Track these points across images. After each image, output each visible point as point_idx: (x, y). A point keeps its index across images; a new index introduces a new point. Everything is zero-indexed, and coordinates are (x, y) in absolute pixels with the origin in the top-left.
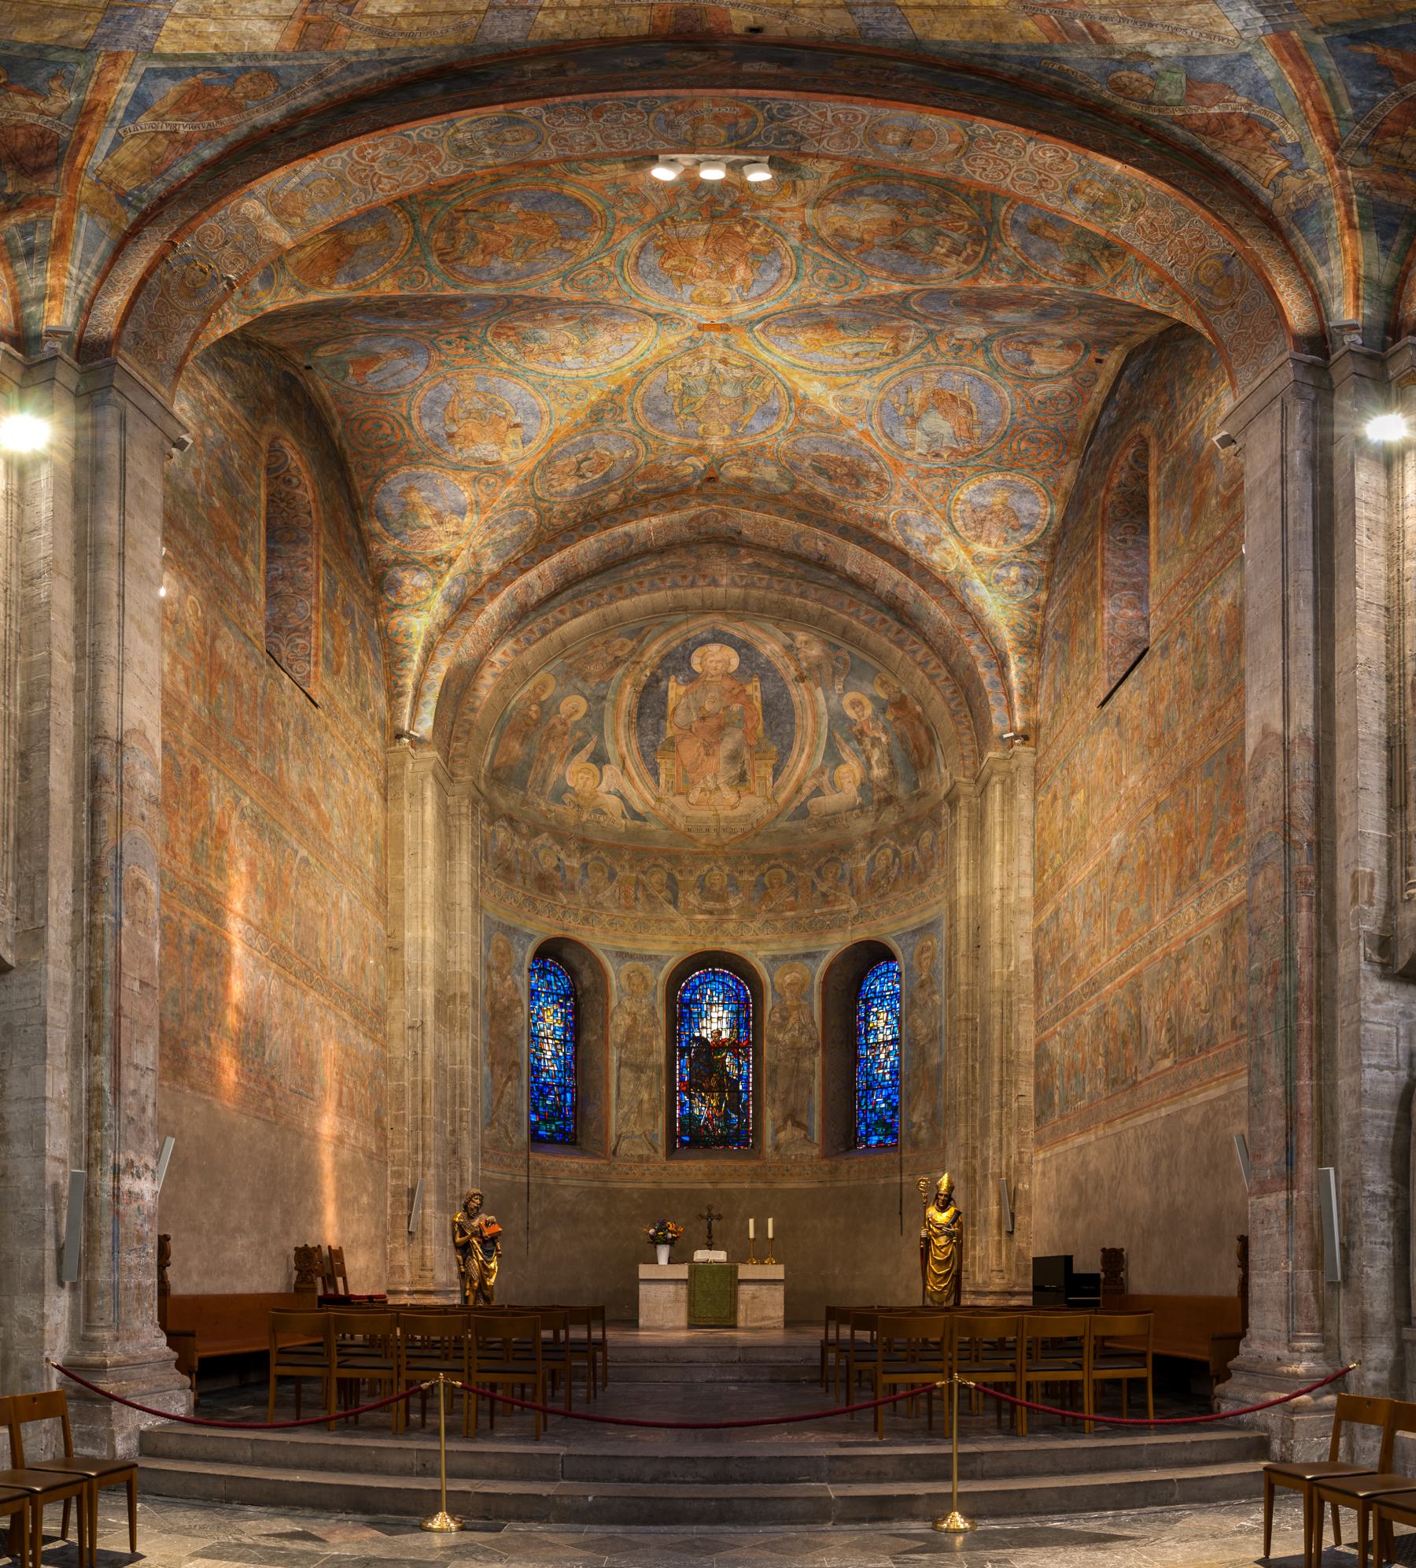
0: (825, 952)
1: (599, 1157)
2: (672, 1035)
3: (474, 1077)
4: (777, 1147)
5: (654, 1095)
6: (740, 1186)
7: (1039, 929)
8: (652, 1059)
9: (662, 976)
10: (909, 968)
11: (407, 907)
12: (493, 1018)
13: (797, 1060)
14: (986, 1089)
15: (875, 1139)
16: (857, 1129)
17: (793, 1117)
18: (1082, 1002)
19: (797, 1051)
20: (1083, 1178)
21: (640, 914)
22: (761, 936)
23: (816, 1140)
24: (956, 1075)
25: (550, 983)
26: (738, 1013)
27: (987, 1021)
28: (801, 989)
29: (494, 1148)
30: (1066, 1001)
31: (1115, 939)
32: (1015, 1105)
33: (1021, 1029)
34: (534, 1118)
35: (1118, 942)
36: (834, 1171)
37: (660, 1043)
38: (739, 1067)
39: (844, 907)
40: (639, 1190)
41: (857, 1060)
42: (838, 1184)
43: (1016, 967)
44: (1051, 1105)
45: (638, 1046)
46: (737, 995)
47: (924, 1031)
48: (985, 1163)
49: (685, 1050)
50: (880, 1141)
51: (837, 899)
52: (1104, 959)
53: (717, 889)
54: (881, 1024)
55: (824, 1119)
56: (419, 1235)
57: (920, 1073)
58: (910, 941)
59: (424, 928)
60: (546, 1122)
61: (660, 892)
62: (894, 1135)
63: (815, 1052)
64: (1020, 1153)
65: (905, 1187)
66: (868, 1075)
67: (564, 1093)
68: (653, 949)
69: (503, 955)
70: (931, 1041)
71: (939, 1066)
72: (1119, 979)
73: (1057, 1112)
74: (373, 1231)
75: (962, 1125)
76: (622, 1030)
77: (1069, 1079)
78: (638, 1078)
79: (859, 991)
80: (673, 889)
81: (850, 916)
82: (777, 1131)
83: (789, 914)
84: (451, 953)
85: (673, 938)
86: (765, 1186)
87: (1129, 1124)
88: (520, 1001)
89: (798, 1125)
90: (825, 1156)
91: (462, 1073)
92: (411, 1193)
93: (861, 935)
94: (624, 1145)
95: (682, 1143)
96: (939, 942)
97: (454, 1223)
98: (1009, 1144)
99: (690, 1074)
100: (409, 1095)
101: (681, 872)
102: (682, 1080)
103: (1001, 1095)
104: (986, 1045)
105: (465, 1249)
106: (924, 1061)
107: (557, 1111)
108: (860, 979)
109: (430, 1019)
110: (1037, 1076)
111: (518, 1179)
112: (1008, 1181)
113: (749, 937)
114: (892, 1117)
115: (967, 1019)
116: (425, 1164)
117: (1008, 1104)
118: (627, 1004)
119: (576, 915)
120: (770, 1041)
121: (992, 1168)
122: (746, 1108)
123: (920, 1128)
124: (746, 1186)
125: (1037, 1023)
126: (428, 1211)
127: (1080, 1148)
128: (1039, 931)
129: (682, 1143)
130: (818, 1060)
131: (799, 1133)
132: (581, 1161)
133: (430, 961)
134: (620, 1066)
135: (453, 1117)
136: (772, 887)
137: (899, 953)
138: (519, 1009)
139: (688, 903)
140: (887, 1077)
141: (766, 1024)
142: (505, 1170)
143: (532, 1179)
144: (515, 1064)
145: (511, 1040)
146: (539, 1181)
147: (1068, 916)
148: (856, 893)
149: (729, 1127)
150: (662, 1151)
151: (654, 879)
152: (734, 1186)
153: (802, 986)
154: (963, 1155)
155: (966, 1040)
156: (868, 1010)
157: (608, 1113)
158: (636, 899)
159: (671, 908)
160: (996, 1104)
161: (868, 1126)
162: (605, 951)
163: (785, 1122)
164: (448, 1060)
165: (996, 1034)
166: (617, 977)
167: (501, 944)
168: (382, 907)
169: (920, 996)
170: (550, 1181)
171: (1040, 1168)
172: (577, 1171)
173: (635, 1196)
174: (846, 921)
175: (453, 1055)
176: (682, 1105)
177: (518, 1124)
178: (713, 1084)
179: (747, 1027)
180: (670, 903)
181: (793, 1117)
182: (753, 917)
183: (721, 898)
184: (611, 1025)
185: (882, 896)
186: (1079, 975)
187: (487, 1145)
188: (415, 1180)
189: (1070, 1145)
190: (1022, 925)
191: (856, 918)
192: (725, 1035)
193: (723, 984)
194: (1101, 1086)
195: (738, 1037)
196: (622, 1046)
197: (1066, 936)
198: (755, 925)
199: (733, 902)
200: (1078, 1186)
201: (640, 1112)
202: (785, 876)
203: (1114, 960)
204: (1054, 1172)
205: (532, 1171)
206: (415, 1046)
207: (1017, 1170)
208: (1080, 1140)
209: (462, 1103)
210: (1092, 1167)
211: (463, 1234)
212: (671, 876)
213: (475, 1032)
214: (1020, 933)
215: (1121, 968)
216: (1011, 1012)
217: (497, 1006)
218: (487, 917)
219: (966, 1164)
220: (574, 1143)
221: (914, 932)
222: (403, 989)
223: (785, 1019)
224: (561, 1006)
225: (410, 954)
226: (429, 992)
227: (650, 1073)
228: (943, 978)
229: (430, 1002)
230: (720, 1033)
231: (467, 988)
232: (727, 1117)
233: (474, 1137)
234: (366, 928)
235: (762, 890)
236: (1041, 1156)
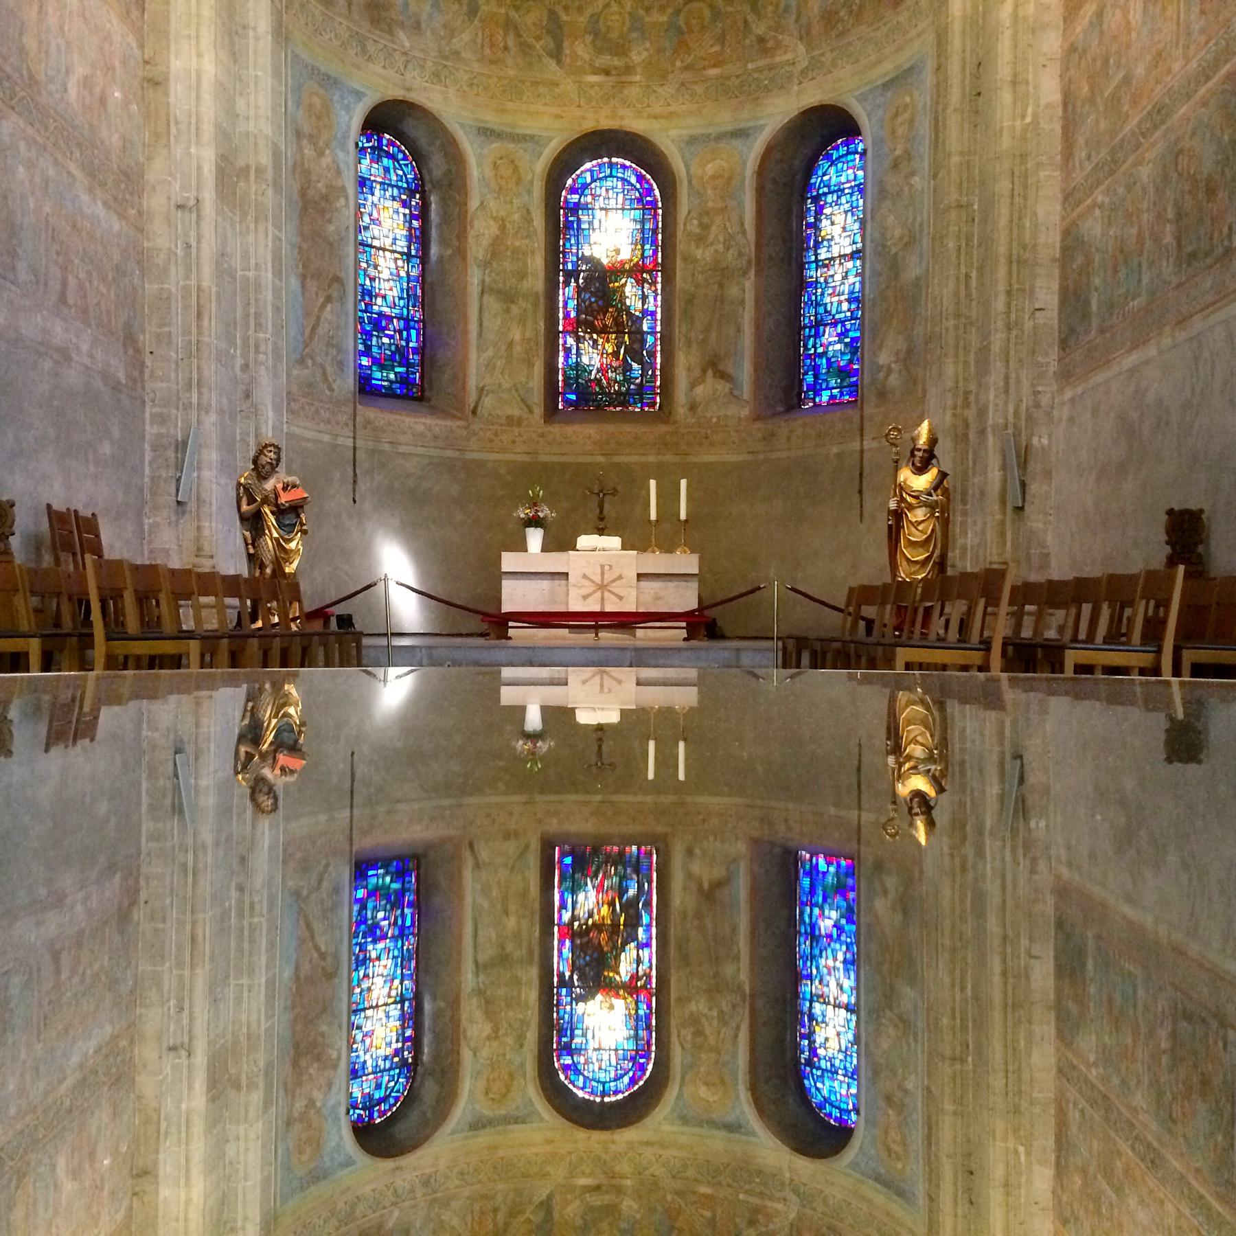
0: (762, 127)
1: (454, 417)
2: (554, 254)
3: (276, 291)
4: (693, 407)
5: (528, 335)
6: (642, 459)
7: (1072, 49)
8: (525, 285)
9: (541, 165)
10: (878, 142)
11: (173, 17)
12: (304, 209)
13: (721, 286)
14: (986, 304)
15: (825, 396)
16: (801, 381)
17: (714, 366)
18: (1139, 145)
19: (722, 273)
20: (1134, 415)
21: (511, 72)
22: (674, 107)
23: (746, 397)
24: (944, 291)
25: (387, 170)
26: (643, 222)
27: (988, 205)
28: (727, 182)
29: (306, 395)
30: (1113, 152)
31: (1196, 27)
32: (1028, 325)
33: (1041, 212)
34: (365, 361)
35: (1202, 31)
36: (769, 438)
37: (538, 263)
38: (644, 298)
39: (788, 57)
40: (507, 462)
41: (802, 284)
42: (774, 456)
43: (1035, 115)
44: (1086, 316)
45: (507, 265)
46: (640, 200)
47: (897, 233)
48: (982, 413)
49: (572, 275)
50: (832, 397)
51: (778, 44)
52: (1177, 66)
53: (614, 35)
54: (837, 230)
55: (756, 367)
56: (192, 506)
57: (890, 294)
58: (880, 100)
59: (199, 55)
60: (382, 367)
61: (538, 38)
62: (854, 389)
63: (745, 273)
64: (1036, 393)
65: (867, 455)
66: (818, 304)
67: (407, 328)
68: (529, 126)
69: (319, 118)
70: (906, 245)
71: (918, 279)
72: (1202, 91)
73: (1095, 322)
74: (120, 497)
75: (949, 361)
76: (485, 242)
77: (1115, 271)
78: (508, 311)
79: (807, 186)
80: (556, 30)
81: (799, 68)
82: (693, 385)
83: (713, 72)
84: (241, 105)
85: (555, 110)
86: (677, 459)
87: (1215, 318)
88: (343, 189)
89: (722, 375)
90: (758, 418)
91: (258, 285)
92: (181, 446)
93: (813, 96)
94: (488, 402)
95: (568, 402)
96: (922, 97)
97: (239, 484)
98: (1018, 382)
99: (578, 309)
100: (178, 306)
101: (566, 8)
102: (567, 315)
103: (1008, 312)
104: (986, 243)
105: (254, 523)
106: (897, 275)
107: (400, 355)
108: (810, 169)
109: (209, 196)
110: (1064, 277)
111: (340, 441)
112: (1017, 434)
113: (657, 109)
114: (851, 362)
115: (960, 206)
116: (203, 408)
117: (1018, 324)
118: (492, 204)
119: (423, 67)
120: (685, 259)
121: (992, 418)
122: (652, 354)
123: (889, 371)
124: (652, 459)
125: (1066, 198)
126: (206, 474)
127: (1132, 371)
128: (1072, 51)
129: (568, 402)
130: (749, 284)
131: (722, 387)
132: (428, 421)
133: (209, 110)
134: (483, 293)
135: (245, 344)
136: (691, 31)
137: (864, 122)
138: (342, 201)
139: (575, 56)
140: (845, 306)
141: (680, 235)
142: (322, 426)
143: (359, 443)
144: (337, 280)
145: (331, 245)
146: (371, 444)
147: (1118, 13)
148: (805, 35)
149: (628, 380)
150: (539, 411)
151: (531, 18)
152: (634, 459)
153: (730, 178)
154: (950, 403)
155: (959, 238)
156: (819, 211)
157: (465, 358)
158: (506, 48)
159: (553, 63)
160: (1000, 324)
161: (816, 377)
162: (462, 125)
163: (704, 371)
164: (237, 263)
165: (1003, 222)
166: (479, 165)
167: (317, 101)
168: (135, 14)
169: (892, 180)
170: (387, 447)
171: (1066, 412)
172: (422, 435)
173: (502, 471)
174: (790, 79)
175: (245, 255)
176: (568, 351)
177: (341, 365)
178: (609, 322)
179: (654, 242)
180: (551, 56)
181: (714, 366)
182: (664, 76)
183: (621, 49)
184: (471, 234)
185: (841, 35)
186: (1135, 103)
187: (295, 389)
188: (186, 430)
189: (1116, 369)
190: (1045, 49)
191: (804, 72)
192: (626, 254)
193: (623, 180)
194: (1167, 269)
195: (643, 257)
196: (486, 265)
197: (1114, 47)
198: (666, 91)
199: (638, 56)
200: (1128, 430)
201: (509, 357)
202: (707, 13)
203: (1194, 64)
204: (1088, 415)
205: (359, 433)
206: (186, 235)
207: (1030, 418)
208: (1133, 359)
209: (259, 327)
210: (1151, 396)
211: (251, 500)
212: (552, 14)
213: (277, 226)
214: (1042, 60)
215: (1205, 74)
216: (1025, 187)
217: (311, 193)
218: (296, 57)
219: (954, 415)
220: (420, 399)
221: (886, 86)
222: (168, 145)
223: (705, 227)
224: (405, 204)
225: (178, 94)
226: (207, 156)
227: (522, 303)
228: (925, 149)
229: (209, 171)
230: (618, 251)
231: (265, 159)
232: (627, 368)
233: (276, 376)
234: (107, 38)
235: (679, 38)
236: (1068, 394)
